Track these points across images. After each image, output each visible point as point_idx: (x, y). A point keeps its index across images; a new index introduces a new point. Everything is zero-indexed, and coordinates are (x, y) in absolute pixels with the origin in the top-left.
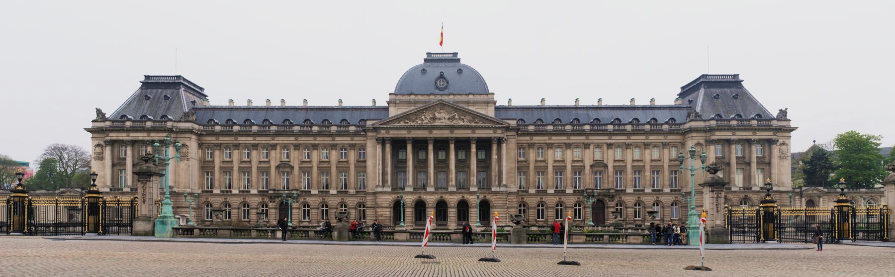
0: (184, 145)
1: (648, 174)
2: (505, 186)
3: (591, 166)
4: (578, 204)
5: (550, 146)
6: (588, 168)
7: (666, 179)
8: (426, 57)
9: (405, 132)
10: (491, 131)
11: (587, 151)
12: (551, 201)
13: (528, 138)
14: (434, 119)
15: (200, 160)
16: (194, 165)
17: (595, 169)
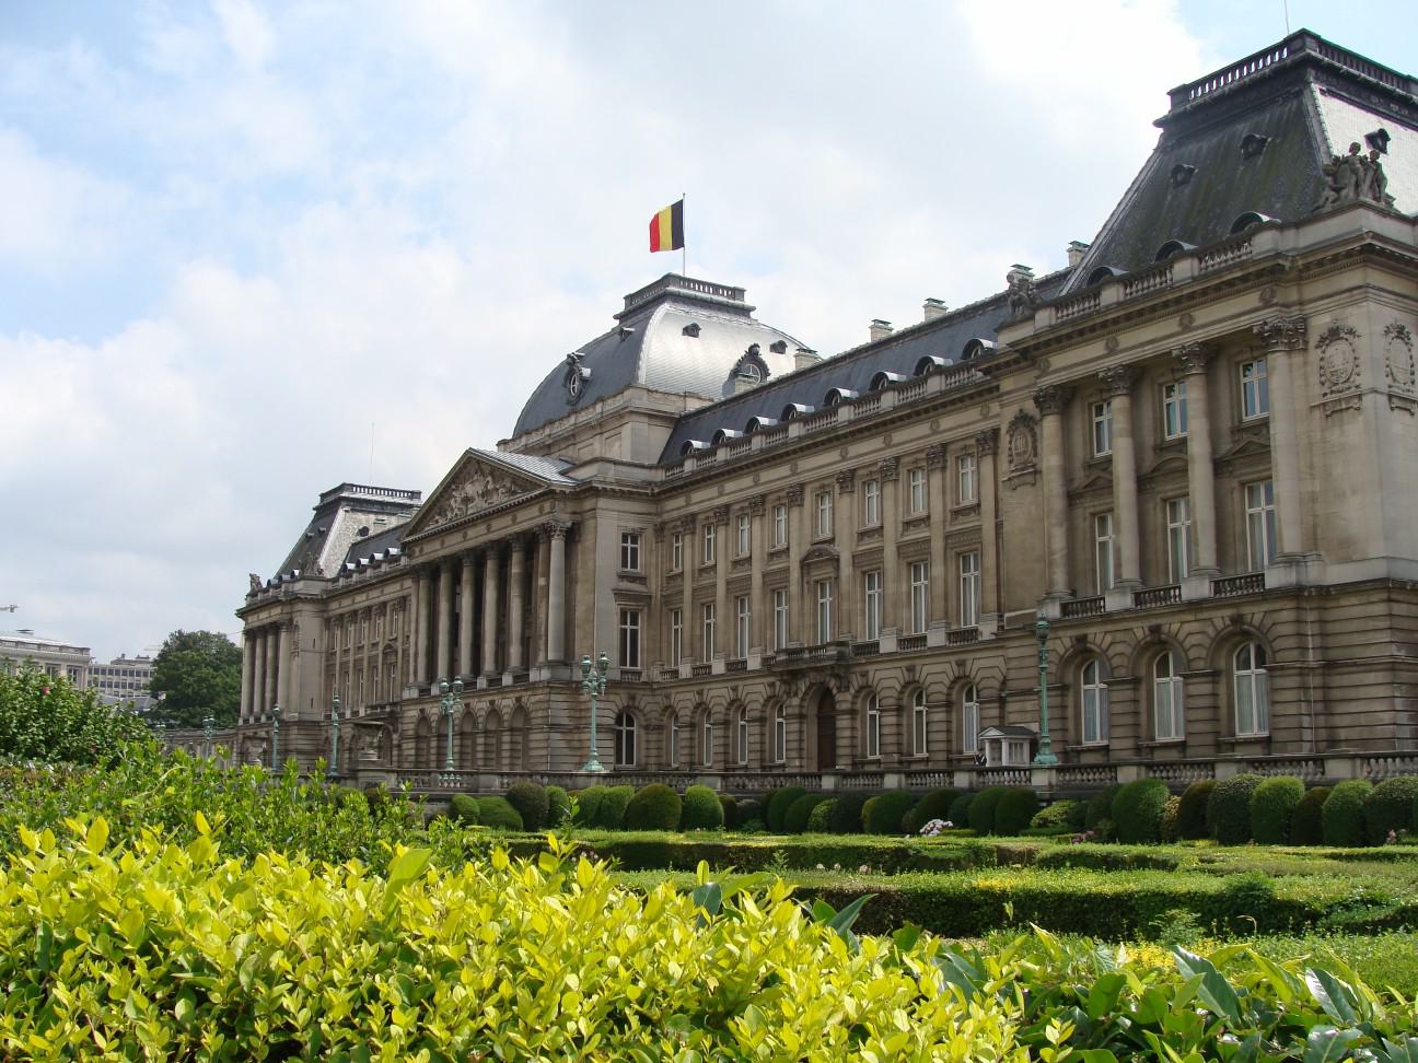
0: (296, 626)
1: (938, 570)
2: (551, 665)
3: (806, 564)
4: (773, 701)
5: (723, 514)
6: (795, 575)
7: (991, 582)
8: (621, 307)
9: (436, 545)
10: (534, 511)
11: (795, 513)
12: (718, 695)
13: (681, 501)
14: (467, 500)
15: (327, 652)
16: (313, 664)
17: (816, 574)
